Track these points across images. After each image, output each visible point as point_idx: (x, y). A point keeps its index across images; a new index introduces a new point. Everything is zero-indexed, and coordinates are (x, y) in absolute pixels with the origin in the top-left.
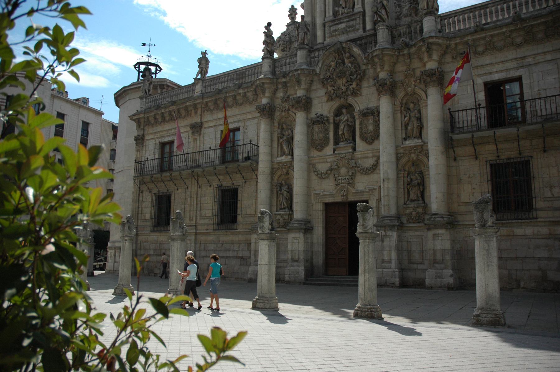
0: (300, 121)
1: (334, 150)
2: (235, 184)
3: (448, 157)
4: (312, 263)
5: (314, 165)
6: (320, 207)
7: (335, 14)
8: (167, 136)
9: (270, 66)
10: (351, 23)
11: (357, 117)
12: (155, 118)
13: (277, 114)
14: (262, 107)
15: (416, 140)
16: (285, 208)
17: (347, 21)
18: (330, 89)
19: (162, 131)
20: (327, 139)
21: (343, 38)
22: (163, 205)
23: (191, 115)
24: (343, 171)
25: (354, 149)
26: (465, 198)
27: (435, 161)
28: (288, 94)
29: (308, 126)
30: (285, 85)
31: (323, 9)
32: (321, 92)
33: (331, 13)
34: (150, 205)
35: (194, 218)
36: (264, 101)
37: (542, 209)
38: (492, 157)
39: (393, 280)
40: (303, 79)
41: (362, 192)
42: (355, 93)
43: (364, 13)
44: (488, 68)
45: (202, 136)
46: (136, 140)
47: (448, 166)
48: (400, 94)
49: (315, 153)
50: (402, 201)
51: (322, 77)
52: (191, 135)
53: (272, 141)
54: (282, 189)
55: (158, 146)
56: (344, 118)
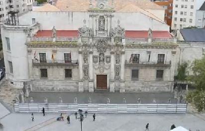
0: (91, 57)
20: (97, 61)
21: (101, 36)
27: (122, 69)
43: (107, 31)
48: (115, 53)
49: (94, 64)
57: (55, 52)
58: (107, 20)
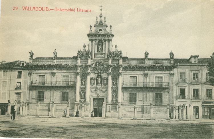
6: (93, 99)
7: (98, 51)
25: (101, 86)
29: (90, 79)
57: (53, 74)
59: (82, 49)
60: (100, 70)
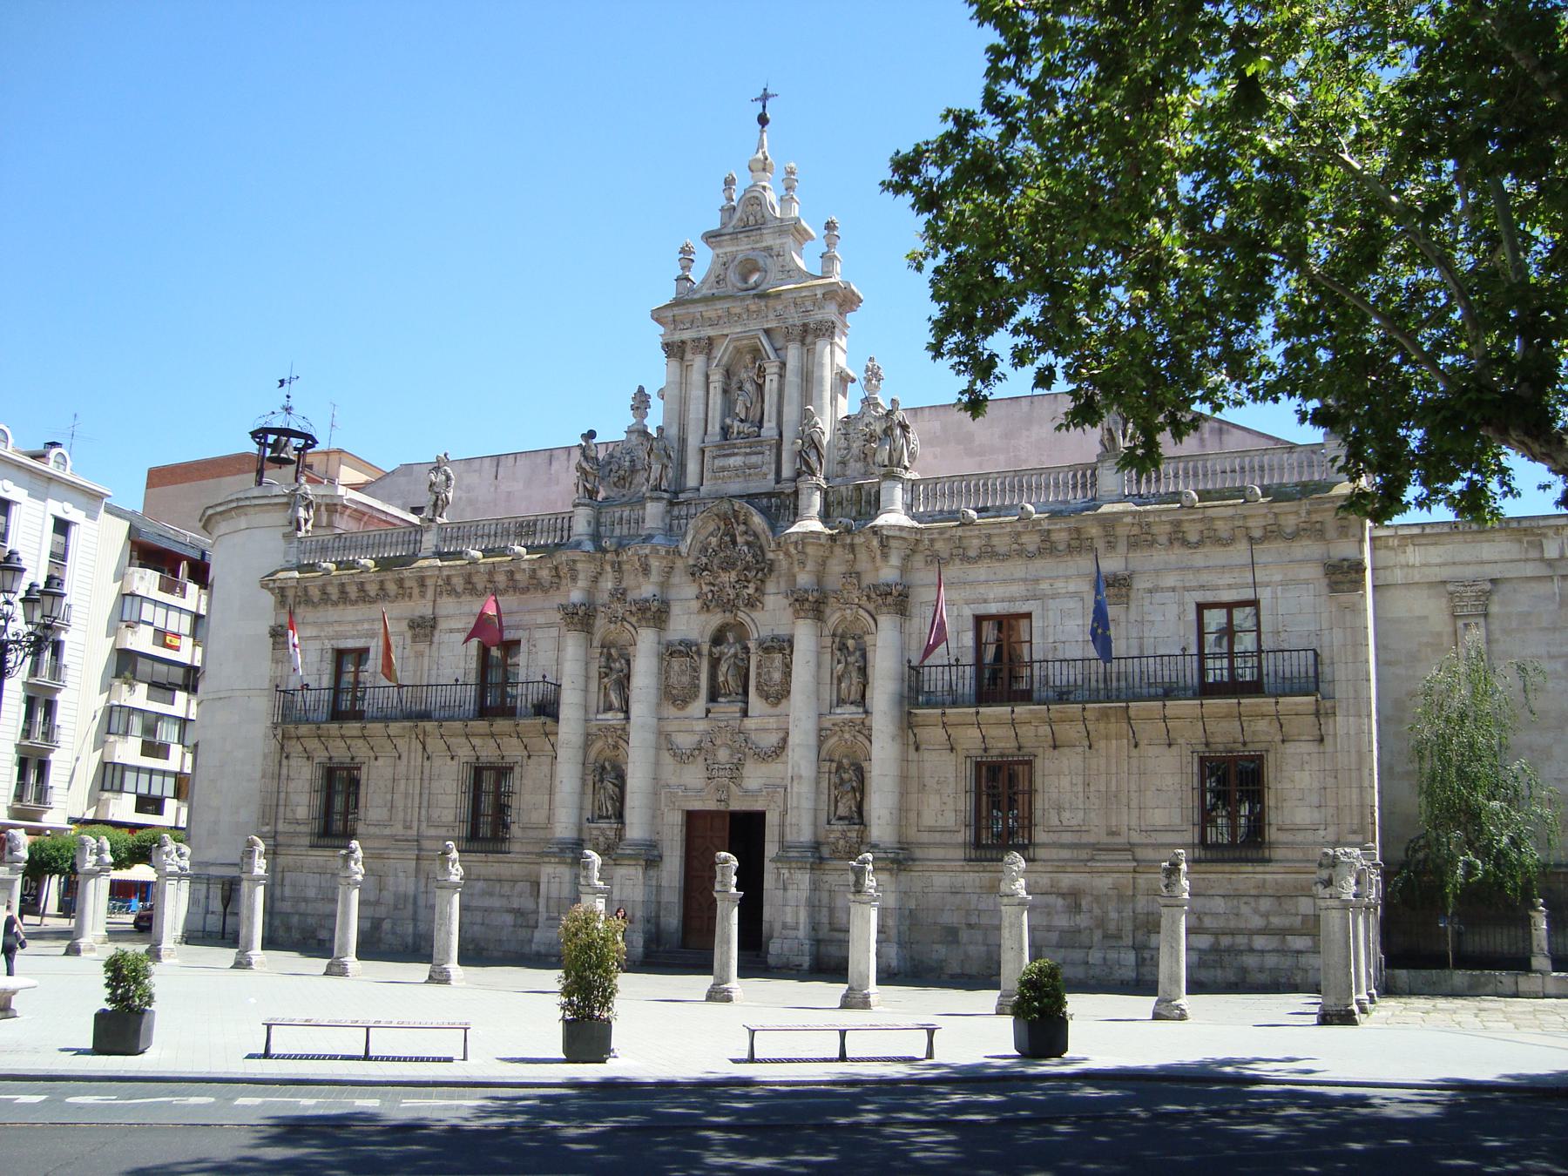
1: (708, 711)
2: (507, 760)
3: (905, 744)
4: (658, 925)
5: (668, 736)
7: (725, 431)
8: (353, 637)
9: (589, 523)
10: (754, 459)
11: (753, 650)
12: (324, 592)
13: (600, 623)
14: (570, 610)
15: (853, 709)
16: (608, 817)
17: (747, 454)
18: (706, 589)
19: (339, 622)
20: (696, 687)
22: (340, 790)
23: (410, 596)
24: (723, 755)
26: (929, 819)
28: (624, 585)
29: (661, 658)
30: (618, 567)
31: (702, 416)
32: (690, 590)
33: (717, 428)
34: (307, 786)
35: (415, 825)
36: (576, 596)
37: (1044, 845)
38: (977, 752)
39: (797, 960)
40: (654, 563)
41: (754, 794)
42: (751, 604)
44: (982, 589)
45: (435, 646)
46: (272, 636)
47: (905, 760)
48: (834, 618)
49: (670, 711)
50: (823, 818)
51: (691, 562)
52: (408, 641)
53: (587, 678)
54: (607, 776)
55: (329, 656)
56: (729, 650)
58: (783, 365)
59: (613, 428)
60: (733, 576)
